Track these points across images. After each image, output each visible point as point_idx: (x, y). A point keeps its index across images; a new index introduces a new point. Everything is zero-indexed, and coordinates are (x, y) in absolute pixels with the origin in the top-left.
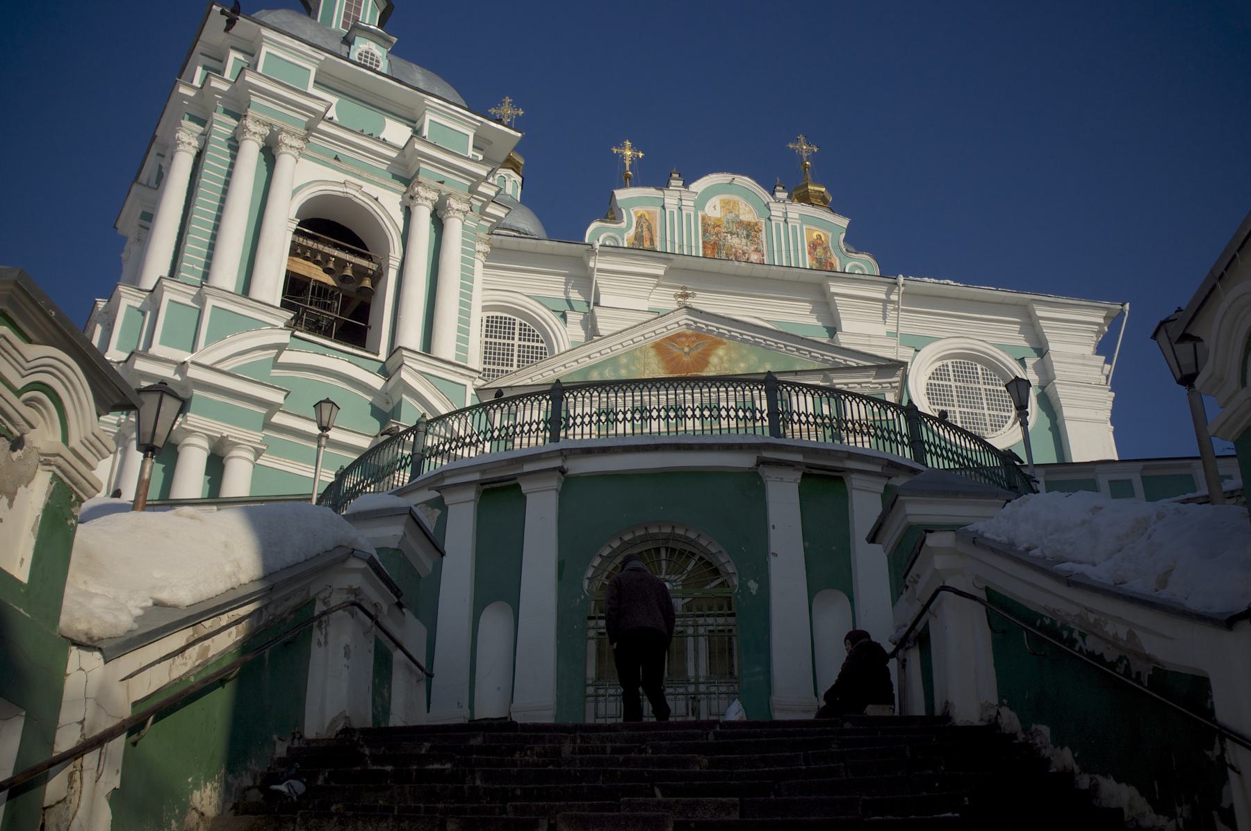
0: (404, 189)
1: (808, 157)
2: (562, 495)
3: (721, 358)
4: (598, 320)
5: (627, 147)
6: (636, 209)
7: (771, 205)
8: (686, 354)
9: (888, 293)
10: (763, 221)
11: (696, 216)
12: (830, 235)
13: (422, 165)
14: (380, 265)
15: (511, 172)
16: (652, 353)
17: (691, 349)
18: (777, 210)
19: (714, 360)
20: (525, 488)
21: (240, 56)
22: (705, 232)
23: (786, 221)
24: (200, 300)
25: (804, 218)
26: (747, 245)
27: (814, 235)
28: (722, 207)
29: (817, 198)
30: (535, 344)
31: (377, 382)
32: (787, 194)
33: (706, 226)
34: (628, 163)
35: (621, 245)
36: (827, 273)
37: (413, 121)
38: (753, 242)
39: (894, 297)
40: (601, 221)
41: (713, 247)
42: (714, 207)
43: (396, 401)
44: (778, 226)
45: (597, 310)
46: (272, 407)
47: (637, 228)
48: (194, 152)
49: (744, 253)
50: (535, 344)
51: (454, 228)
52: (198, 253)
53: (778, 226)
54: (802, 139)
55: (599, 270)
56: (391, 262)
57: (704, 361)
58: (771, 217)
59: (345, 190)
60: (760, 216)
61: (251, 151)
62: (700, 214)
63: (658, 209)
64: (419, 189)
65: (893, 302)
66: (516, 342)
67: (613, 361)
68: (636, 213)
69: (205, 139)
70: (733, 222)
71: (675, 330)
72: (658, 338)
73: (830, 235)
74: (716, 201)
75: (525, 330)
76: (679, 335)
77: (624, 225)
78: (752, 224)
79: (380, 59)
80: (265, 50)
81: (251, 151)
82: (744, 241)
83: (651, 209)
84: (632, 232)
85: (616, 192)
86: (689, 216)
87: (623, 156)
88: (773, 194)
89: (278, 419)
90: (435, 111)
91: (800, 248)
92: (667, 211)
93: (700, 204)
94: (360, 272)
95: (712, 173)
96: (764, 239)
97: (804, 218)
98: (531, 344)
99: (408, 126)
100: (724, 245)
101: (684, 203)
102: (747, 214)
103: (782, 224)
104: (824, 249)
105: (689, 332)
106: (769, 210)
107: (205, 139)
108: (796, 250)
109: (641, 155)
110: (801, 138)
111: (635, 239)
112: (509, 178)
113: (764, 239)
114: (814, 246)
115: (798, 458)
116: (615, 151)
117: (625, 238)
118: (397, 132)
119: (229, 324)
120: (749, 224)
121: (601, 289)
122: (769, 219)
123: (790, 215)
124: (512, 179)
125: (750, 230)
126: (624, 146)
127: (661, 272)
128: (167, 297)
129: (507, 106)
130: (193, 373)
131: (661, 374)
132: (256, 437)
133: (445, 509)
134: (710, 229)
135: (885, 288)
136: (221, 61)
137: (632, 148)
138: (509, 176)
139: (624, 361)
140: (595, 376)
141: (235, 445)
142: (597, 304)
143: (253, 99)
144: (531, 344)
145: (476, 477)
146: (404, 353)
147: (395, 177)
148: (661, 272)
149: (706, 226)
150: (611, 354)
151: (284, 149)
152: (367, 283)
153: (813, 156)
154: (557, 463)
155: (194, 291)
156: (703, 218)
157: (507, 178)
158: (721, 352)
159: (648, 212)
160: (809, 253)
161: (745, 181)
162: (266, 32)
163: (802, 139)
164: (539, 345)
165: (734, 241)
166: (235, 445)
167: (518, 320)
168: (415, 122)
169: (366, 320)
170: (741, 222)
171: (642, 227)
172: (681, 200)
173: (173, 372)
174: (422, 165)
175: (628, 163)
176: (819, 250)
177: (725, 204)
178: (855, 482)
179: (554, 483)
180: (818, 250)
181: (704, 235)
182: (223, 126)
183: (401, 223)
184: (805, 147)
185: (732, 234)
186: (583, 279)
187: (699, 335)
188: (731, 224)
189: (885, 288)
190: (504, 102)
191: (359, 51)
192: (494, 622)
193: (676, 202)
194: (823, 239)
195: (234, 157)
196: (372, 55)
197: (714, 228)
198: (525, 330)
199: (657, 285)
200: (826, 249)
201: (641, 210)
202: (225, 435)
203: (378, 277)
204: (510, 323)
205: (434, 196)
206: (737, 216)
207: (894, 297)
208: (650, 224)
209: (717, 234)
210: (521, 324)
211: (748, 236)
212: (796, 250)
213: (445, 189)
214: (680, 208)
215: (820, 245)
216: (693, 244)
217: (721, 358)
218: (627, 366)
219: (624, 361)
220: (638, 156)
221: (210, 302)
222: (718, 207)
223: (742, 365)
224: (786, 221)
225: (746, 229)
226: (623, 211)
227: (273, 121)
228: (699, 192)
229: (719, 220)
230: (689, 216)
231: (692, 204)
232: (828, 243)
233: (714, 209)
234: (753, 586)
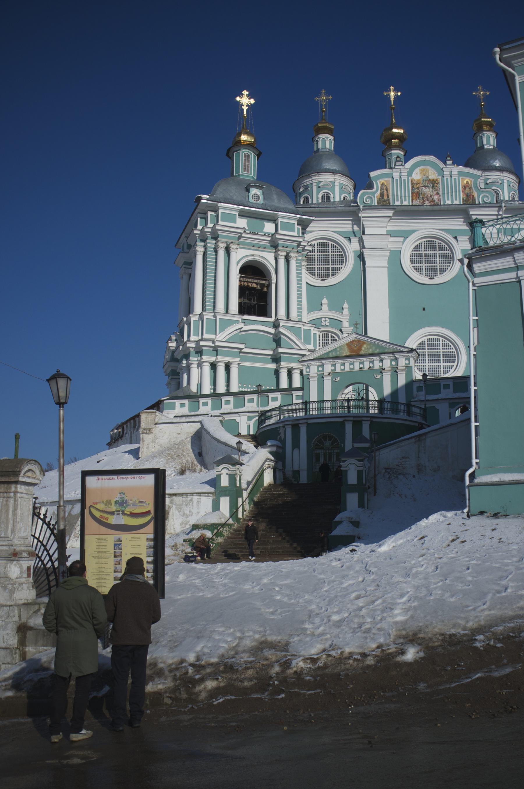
0: (274, 251)
1: (483, 99)
2: (307, 427)
3: (365, 348)
4: (364, 241)
5: (392, 90)
6: (380, 180)
7: (444, 169)
8: (355, 347)
9: (498, 211)
10: (440, 177)
11: (408, 180)
12: (473, 180)
13: (279, 242)
14: (269, 283)
15: (328, 135)
16: (346, 347)
17: (357, 345)
18: (447, 173)
19: (363, 349)
20: (300, 425)
21: (213, 213)
22: (412, 187)
23: (451, 176)
24: (215, 316)
25: (460, 174)
26: (432, 192)
27: (465, 182)
28: (420, 173)
29: (487, 125)
30: (338, 253)
31: (272, 331)
32: (452, 161)
33: (413, 184)
34: (392, 100)
35: (373, 204)
36: (468, 206)
37: (274, 220)
38: (435, 190)
39: (501, 213)
40: (364, 189)
41: (417, 194)
42: (417, 174)
43: (279, 337)
44: (447, 179)
45: (364, 237)
46: (241, 349)
47: (381, 190)
48: (202, 253)
49: (431, 196)
50: (338, 253)
51: (293, 264)
52: (210, 295)
53: (447, 179)
54: (480, 88)
55: (363, 217)
56: (272, 282)
57: (361, 350)
58: (444, 176)
59: (254, 258)
60: (439, 175)
61: (221, 253)
62: (410, 178)
63: (390, 179)
64: (279, 252)
65: (500, 215)
66: (330, 253)
67: (335, 350)
68: (380, 182)
69: (205, 247)
70: (426, 180)
71: (352, 339)
72: (348, 342)
73: (473, 180)
74: (417, 170)
75: (334, 247)
76: (353, 341)
77: (374, 190)
78: (435, 180)
79: (260, 196)
80: (220, 211)
81: (221, 253)
82: (431, 189)
83: (387, 179)
84: (379, 193)
85: (371, 173)
86: (404, 180)
87: (390, 96)
88: (445, 163)
89: (245, 350)
90: (282, 217)
91: (457, 190)
92: (395, 179)
93: (410, 174)
94: (262, 286)
95: (415, 156)
96: (441, 187)
97: (460, 174)
98: (336, 253)
99: (274, 223)
100: (421, 193)
101: (402, 174)
102: (433, 175)
103: (449, 178)
104: (470, 188)
105: (356, 340)
106: (443, 171)
107: (205, 247)
108: (456, 192)
109: (399, 93)
110: (480, 88)
111: (380, 196)
112: (327, 139)
113: (441, 187)
114: (465, 187)
115: (352, 419)
116: (385, 94)
117: (376, 196)
118: (269, 227)
119: (225, 324)
120: (433, 180)
121: (365, 226)
122: (443, 176)
123: (453, 173)
124: (329, 139)
125: (434, 183)
126: (390, 91)
127: (391, 215)
128: (205, 318)
129: (323, 95)
130: (217, 344)
131: (349, 354)
132: (237, 360)
133: (286, 429)
134: (415, 186)
135: (497, 209)
136: (205, 214)
137: (394, 91)
138: (327, 138)
139: (338, 349)
140: (331, 355)
141: (232, 363)
142: (363, 233)
143: (219, 233)
144: (336, 253)
145: (290, 423)
146: (280, 321)
147: (271, 246)
148: (391, 215)
149: (413, 184)
150: (335, 348)
151: (232, 250)
152: (265, 289)
153: (486, 98)
154: (305, 421)
155: (213, 314)
156: (412, 181)
157: (326, 139)
158: (365, 346)
159: (386, 181)
160: (462, 192)
161: (431, 158)
162: (220, 204)
163: (480, 88)
164: (340, 253)
165: (427, 191)
166: (232, 363)
167: (330, 243)
168: (275, 221)
169: (266, 302)
170: (430, 180)
171: (383, 189)
172: (401, 172)
173: (211, 343)
174: (279, 242)
175: (392, 100)
176: (467, 189)
177: (422, 170)
178: (363, 422)
179: (305, 425)
180: (467, 189)
181: (412, 189)
182: (211, 243)
183: (274, 265)
184: (482, 93)
185: (425, 186)
186: (357, 221)
187: (359, 341)
188: (425, 182)
189: (497, 209)
190: (322, 93)
191: (252, 195)
192: (296, 451)
193: (398, 174)
194: (469, 183)
195: (216, 255)
196: (257, 195)
197: (417, 185)
198: (334, 247)
199: (390, 219)
200: (470, 188)
201: (383, 181)
202: (229, 360)
203: (269, 286)
204: (327, 245)
205: (285, 254)
206: (428, 177)
207: (501, 213)
208: (387, 187)
209: (418, 188)
210: (332, 245)
211: (433, 187)
212: (456, 192)
213: (288, 249)
214: (400, 177)
215: (468, 186)
216: (407, 195)
217: (365, 348)
218: (339, 351)
219: (338, 349)
220: (398, 94)
221: (218, 317)
222: (419, 174)
223: (371, 350)
224: (451, 176)
225: (432, 183)
226: (374, 182)
227: (227, 240)
228: (409, 167)
229: (419, 180)
230: (404, 180)
231: (406, 174)
232: (471, 185)
233: (417, 176)
234: (342, 445)
